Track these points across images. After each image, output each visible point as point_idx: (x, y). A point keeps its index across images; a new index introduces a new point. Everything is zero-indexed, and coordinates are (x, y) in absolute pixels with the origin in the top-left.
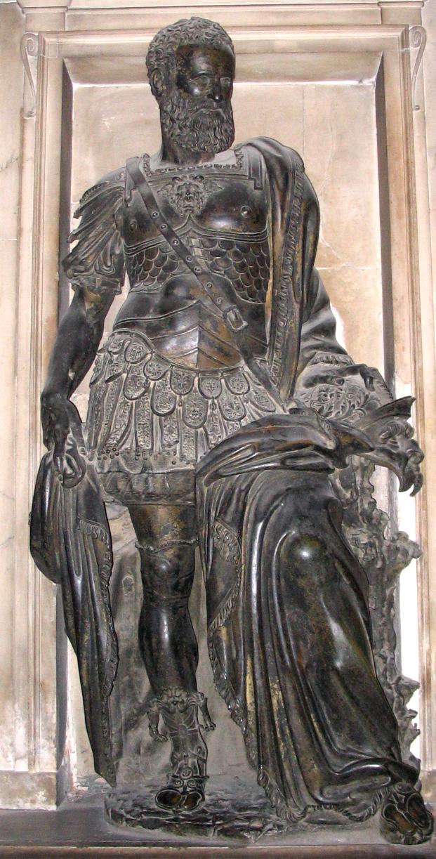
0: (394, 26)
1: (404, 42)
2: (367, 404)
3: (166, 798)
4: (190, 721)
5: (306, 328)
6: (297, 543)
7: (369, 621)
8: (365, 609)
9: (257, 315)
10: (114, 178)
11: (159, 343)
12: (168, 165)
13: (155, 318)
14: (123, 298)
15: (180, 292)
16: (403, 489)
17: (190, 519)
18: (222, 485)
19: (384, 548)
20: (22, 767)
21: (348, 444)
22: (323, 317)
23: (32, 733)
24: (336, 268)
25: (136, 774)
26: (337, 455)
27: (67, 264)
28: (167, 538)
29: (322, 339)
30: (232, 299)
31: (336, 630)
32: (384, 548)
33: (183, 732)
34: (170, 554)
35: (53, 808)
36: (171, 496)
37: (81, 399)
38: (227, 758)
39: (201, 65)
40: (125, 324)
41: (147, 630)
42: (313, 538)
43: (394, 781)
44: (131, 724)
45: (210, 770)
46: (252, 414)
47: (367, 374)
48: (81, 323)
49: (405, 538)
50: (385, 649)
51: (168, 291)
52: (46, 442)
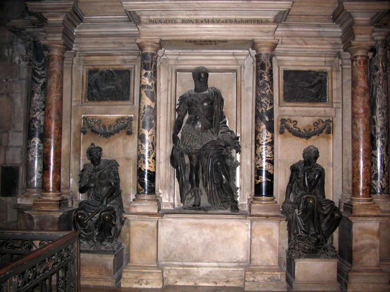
0: (239, 65)
1: (241, 68)
2: (231, 138)
3: (194, 206)
4: (198, 193)
5: (220, 123)
6: (217, 162)
7: (231, 177)
8: (229, 174)
9: (212, 121)
10: (186, 94)
11: (194, 126)
12: (196, 93)
13: (193, 121)
14: (187, 117)
15: (198, 117)
16: (237, 153)
17: (199, 157)
18: (205, 152)
20: (167, 201)
21: (227, 145)
22: (224, 120)
23: (169, 195)
25: (188, 203)
26: (225, 147)
27: (176, 110)
28: (195, 161)
29: (224, 125)
30: (207, 119)
31: (224, 177)
33: (197, 195)
34: (195, 164)
35: (173, 209)
36: (196, 153)
37: (179, 135)
38: (204, 201)
39: (202, 75)
40: (188, 122)
41: (191, 177)
42: (220, 161)
43: (233, 202)
44: (187, 194)
45: (201, 202)
46: (210, 139)
47: (232, 132)
48: (179, 121)
49: (237, 161)
50: (233, 181)
51: (196, 117)
52: (173, 143)
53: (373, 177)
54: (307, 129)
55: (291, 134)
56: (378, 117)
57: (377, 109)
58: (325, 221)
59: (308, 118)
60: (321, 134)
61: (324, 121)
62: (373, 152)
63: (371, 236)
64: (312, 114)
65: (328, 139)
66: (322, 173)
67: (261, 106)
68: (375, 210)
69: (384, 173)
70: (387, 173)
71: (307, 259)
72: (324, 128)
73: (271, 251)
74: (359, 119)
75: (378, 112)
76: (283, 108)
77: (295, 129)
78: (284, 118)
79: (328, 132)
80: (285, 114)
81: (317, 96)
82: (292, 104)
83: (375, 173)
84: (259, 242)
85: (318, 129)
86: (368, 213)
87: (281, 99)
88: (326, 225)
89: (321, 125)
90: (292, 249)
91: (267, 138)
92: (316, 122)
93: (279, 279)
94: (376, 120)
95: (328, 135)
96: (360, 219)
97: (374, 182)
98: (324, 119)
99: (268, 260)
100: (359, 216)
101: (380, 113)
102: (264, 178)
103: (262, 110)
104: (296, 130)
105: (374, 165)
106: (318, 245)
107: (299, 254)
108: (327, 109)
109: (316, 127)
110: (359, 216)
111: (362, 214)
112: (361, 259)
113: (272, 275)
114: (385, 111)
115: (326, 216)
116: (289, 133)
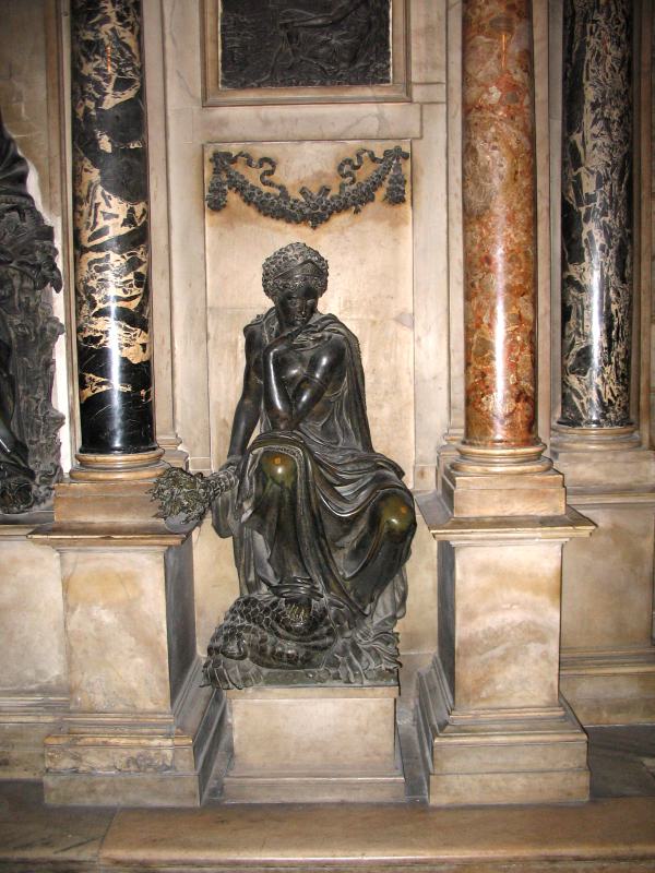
19: (38, 329)
24: (34, 134)
32: (38, 329)
49: (56, 321)
53: (570, 363)
54: (314, 189)
55: (252, 211)
56: (588, 135)
57: (587, 107)
58: (351, 540)
59: (317, 146)
60: (370, 208)
61: (379, 155)
62: (573, 271)
63: (528, 596)
64: (336, 130)
65: (396, 223)
66: (344, 356)
67: (84, 93)
68: (545, 494)
69: (610, 349)
70: (619, 348)
71: (277, 691)
72: (377, 183)
73: (139, 660)
74: (485, 128)
75: (588, 118)
76: (221, 112)
77: (265, 189)
78: (224, 148)
79: (396, 198)
80: (226, 133)
81: (354, 60)
82: (251, 95)
83: (577, 349)
84: (91, 626)
85: (354, 187)
86: (519, 508)
87: (211, 77)
88: (355, 554)
89: (367, 171)
90: (217, 650)
91: (107, 223)
92: (349, 161)
93: (169, 764)
94: (581, 149)
95: (396, 209)
96: (479, 533)
97: (573, 380)
98: (378, 149)
99: (133, 692)
100: (479, 523)
101: (595, 122)
102: (116, 385)
103: (87, 110)
104: (268, 195)
105: (573, 321)
106: (315, 638)
107: (243, 670)
108: (390, 110)
109: (349, 179)
110: (479, 523)
111: (491, 511)
112: (490, 681)
113: (141, 751)
114: (615, 115)
115: (351, 522)
116: (244, 206)
